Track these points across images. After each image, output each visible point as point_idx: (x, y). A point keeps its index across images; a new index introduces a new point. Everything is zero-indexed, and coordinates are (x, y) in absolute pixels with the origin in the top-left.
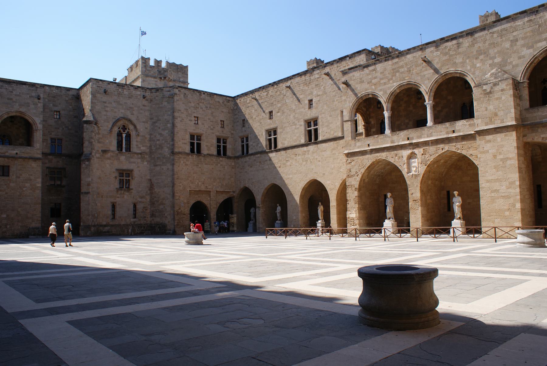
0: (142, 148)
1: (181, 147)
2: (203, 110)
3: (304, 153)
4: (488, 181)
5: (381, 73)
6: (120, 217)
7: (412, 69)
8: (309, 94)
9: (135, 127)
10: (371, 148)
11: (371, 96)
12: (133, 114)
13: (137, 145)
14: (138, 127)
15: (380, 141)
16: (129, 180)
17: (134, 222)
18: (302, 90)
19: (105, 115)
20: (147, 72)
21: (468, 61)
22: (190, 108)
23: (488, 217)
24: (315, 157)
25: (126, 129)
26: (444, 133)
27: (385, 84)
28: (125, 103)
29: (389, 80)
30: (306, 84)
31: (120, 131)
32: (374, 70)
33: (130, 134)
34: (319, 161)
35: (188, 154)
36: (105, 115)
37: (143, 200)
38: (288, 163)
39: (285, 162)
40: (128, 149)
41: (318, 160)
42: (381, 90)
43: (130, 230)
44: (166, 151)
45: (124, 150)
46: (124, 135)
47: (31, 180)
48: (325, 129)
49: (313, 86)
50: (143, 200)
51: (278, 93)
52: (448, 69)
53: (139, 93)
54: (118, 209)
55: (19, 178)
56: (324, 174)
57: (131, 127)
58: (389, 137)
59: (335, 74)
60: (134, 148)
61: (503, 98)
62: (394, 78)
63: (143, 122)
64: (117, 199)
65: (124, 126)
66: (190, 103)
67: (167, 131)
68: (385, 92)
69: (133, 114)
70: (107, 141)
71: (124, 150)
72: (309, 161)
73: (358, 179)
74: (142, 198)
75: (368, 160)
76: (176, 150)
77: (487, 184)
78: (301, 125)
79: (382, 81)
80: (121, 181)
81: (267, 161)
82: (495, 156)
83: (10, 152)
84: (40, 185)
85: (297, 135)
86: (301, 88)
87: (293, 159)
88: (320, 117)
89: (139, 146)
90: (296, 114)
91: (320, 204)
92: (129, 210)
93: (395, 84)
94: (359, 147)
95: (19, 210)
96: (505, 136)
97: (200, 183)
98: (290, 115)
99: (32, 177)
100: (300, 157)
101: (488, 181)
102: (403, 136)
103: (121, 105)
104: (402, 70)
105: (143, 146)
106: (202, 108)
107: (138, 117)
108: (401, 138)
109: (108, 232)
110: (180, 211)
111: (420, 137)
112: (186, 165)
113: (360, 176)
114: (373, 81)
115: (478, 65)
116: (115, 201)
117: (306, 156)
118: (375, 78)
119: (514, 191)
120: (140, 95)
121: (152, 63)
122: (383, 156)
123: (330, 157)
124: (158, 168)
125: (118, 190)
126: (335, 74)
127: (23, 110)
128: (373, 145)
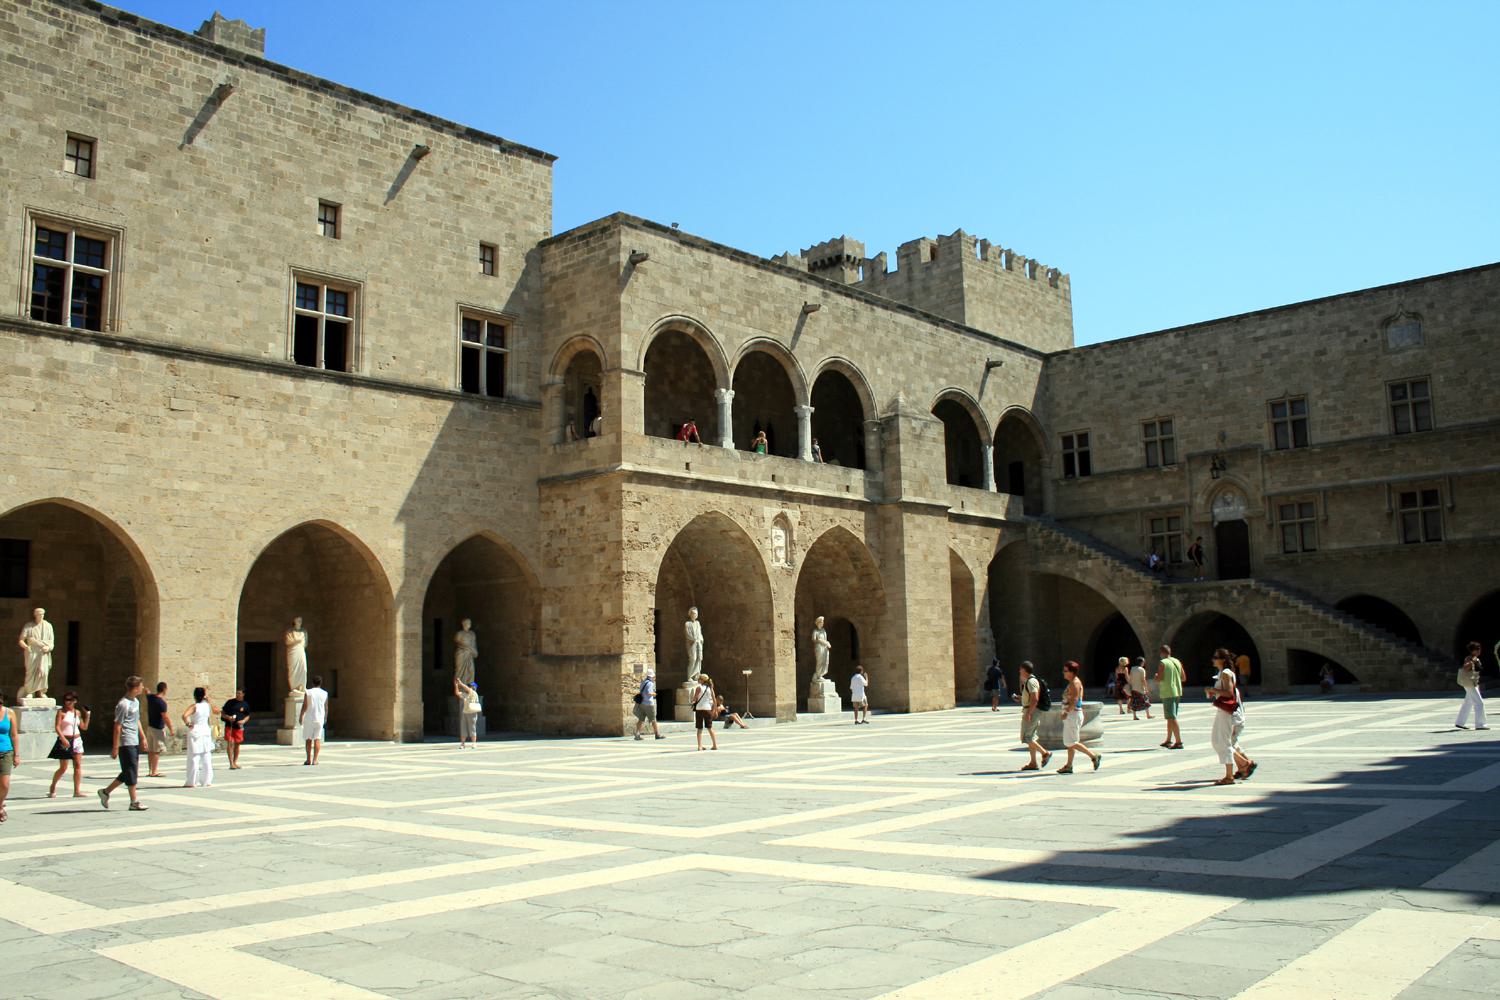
3: (282, 403)
4: (918, 602)
5: (723, 285)
7: (783, 315)
8: (327, 180)
10: (694, 475)
11: (690, 331)
15: (715, 462)
18: (292, 143)
21: (866, 353)
23: (919, 672)
24: (339, 435)
26: (835, 486)
27: (730, 318)
29: (740, 314)
30: (309, 126)
32: (706, 266)
34: (355, 455)
38: (183, 425)
39: (161, 411)
41: (350, 448)
42: (721, 329)
48: (390, 341)
49: (352, 158)
51: (144, 78)
52: (840, 352)
56: (374, 510)
58: (736, 461)
59: (446, 171)
61: (935, 454)
62: (749, 313)
68: (729, 340)
72: (302, 440)
73: (659, 556)
75: (688, 506)
77: (917, 608)
78: (270, 282)
79: (724, 308)
81: (26, 371)
82: (926, 557)
85: (250, 315)
86: (290, 133)
87: (213, 409)
88: (370, 287)
90: (249, 222)
91: (298, 622)
93: (750, 330)
94: (662, 463)
96: (938, 522)
98: (211, 213)
100: (254, 413)
101: (918, 602)
102: (763, 467)
104: (765, 305)
108: (760, 469)
111: (794, 482)
113: (664, 549)
114: (705, 295)
115: (880, 372)
117: (292, 417)
118: (709, 289)
119: (947, 624)
122: (723, 503)
123: (407, 453)
126: (446, 171)
128: (699, 470)
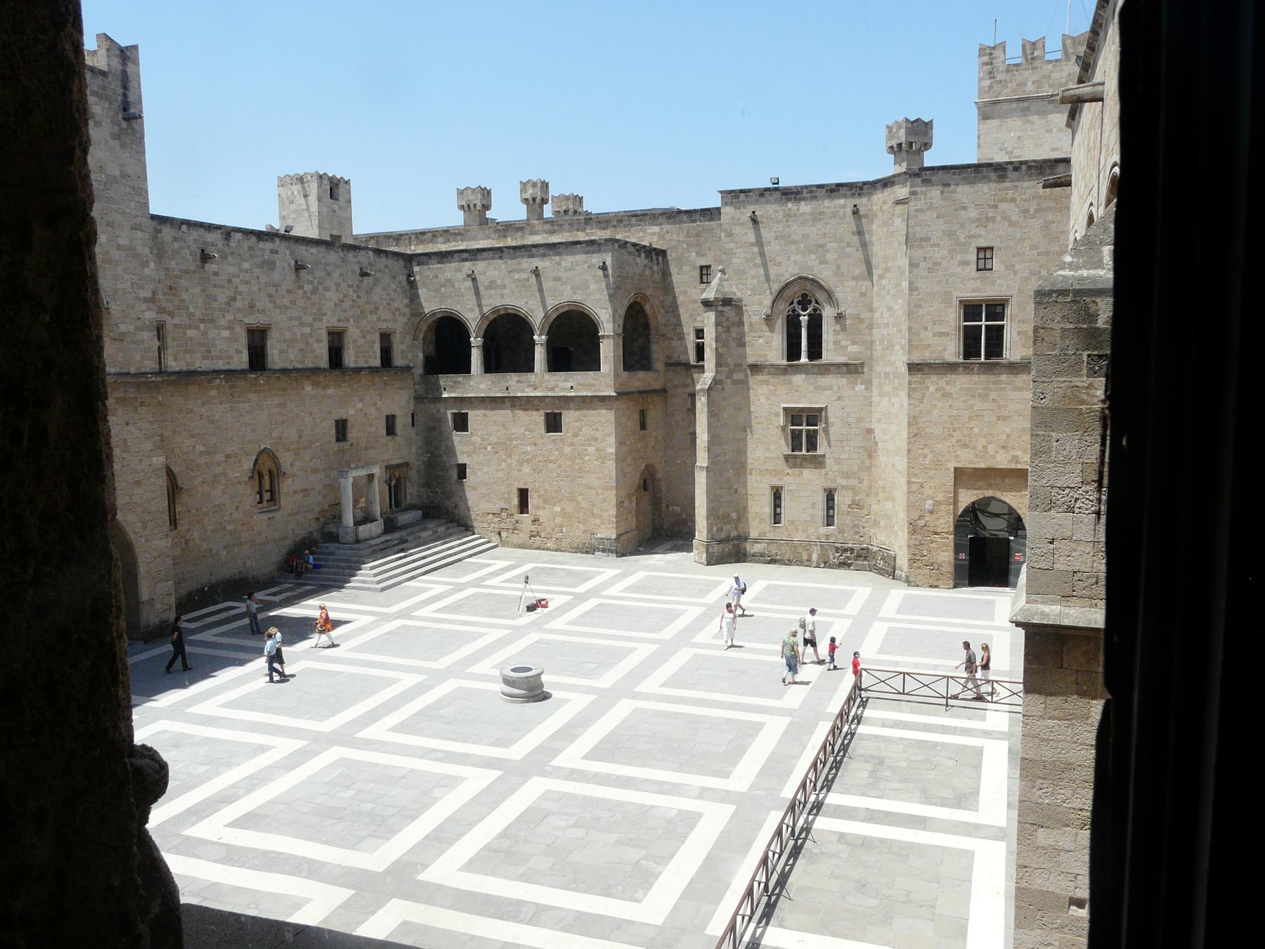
0: (850, 349)
1: (929, 346)
2: (1013, 224)
6: (793, 522)
9: (830, 296)
12: (826, 262)
13: (835, 343)
14: (839, 294)
16: (816, 431)
17: (828, 536)
19: (753, 277)
20: (997, 88)
22: (962, 226)
25: (810, 302)
28: (806, 236)
31: (794, 310)
33: (820, 317)
35: (951, 367)
36: (753, 277)
37: (853, 482)
40: (815, 352)
43: (815, 557)
44: (900, 359)
45: (804, 359)
46: (804, 319)
47: (596, 439)
50: (853, 482)
53: (842, 201)
54: (785, 502)
55: (576, 435)
57: (821, 296)
60: (829, 354)
63: (853, 278)
64: (786, 479)
65: (804, 296)
66: (965, 208)
67: (900, 301)
69: (826, 262)
70: (761, 341)
71: (804, 359)
74: (848, 478)
76: (916, 359)
80: (796, 437)
83: (561, 385)
84: (612, 450)
89: (843, 343)
92: (814, 506)
95: (580, 498)
97: (991, 448)
99: (599, 435)
103: (795, 242)
105: (854, 343)
106: (1005, 218)
107: (838, 267)
109: (762, 555)
110: (921, 523)
112: (946, 395)
116: (779, 483)
120: (844, 206)
121: (1014, 53)
124: (885, 402)
125: (787, 458)
127: (578, 297)
